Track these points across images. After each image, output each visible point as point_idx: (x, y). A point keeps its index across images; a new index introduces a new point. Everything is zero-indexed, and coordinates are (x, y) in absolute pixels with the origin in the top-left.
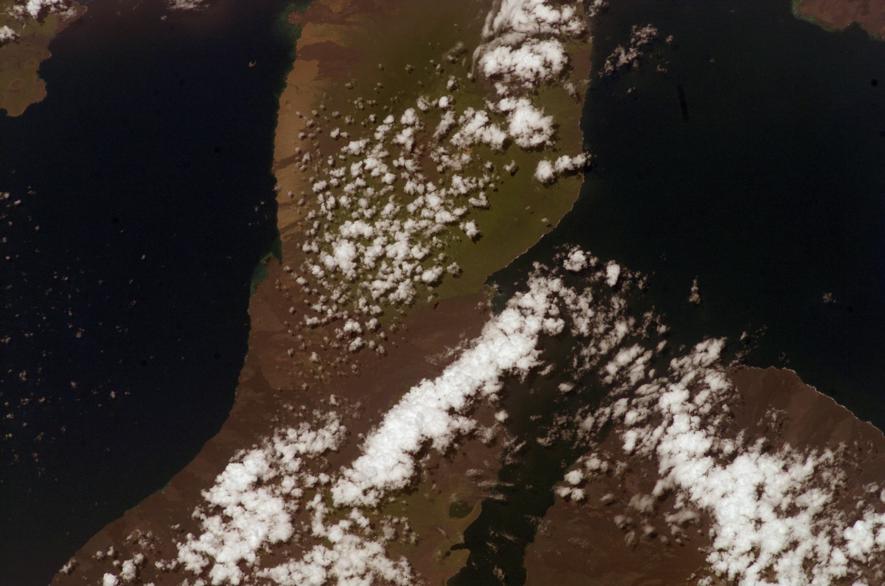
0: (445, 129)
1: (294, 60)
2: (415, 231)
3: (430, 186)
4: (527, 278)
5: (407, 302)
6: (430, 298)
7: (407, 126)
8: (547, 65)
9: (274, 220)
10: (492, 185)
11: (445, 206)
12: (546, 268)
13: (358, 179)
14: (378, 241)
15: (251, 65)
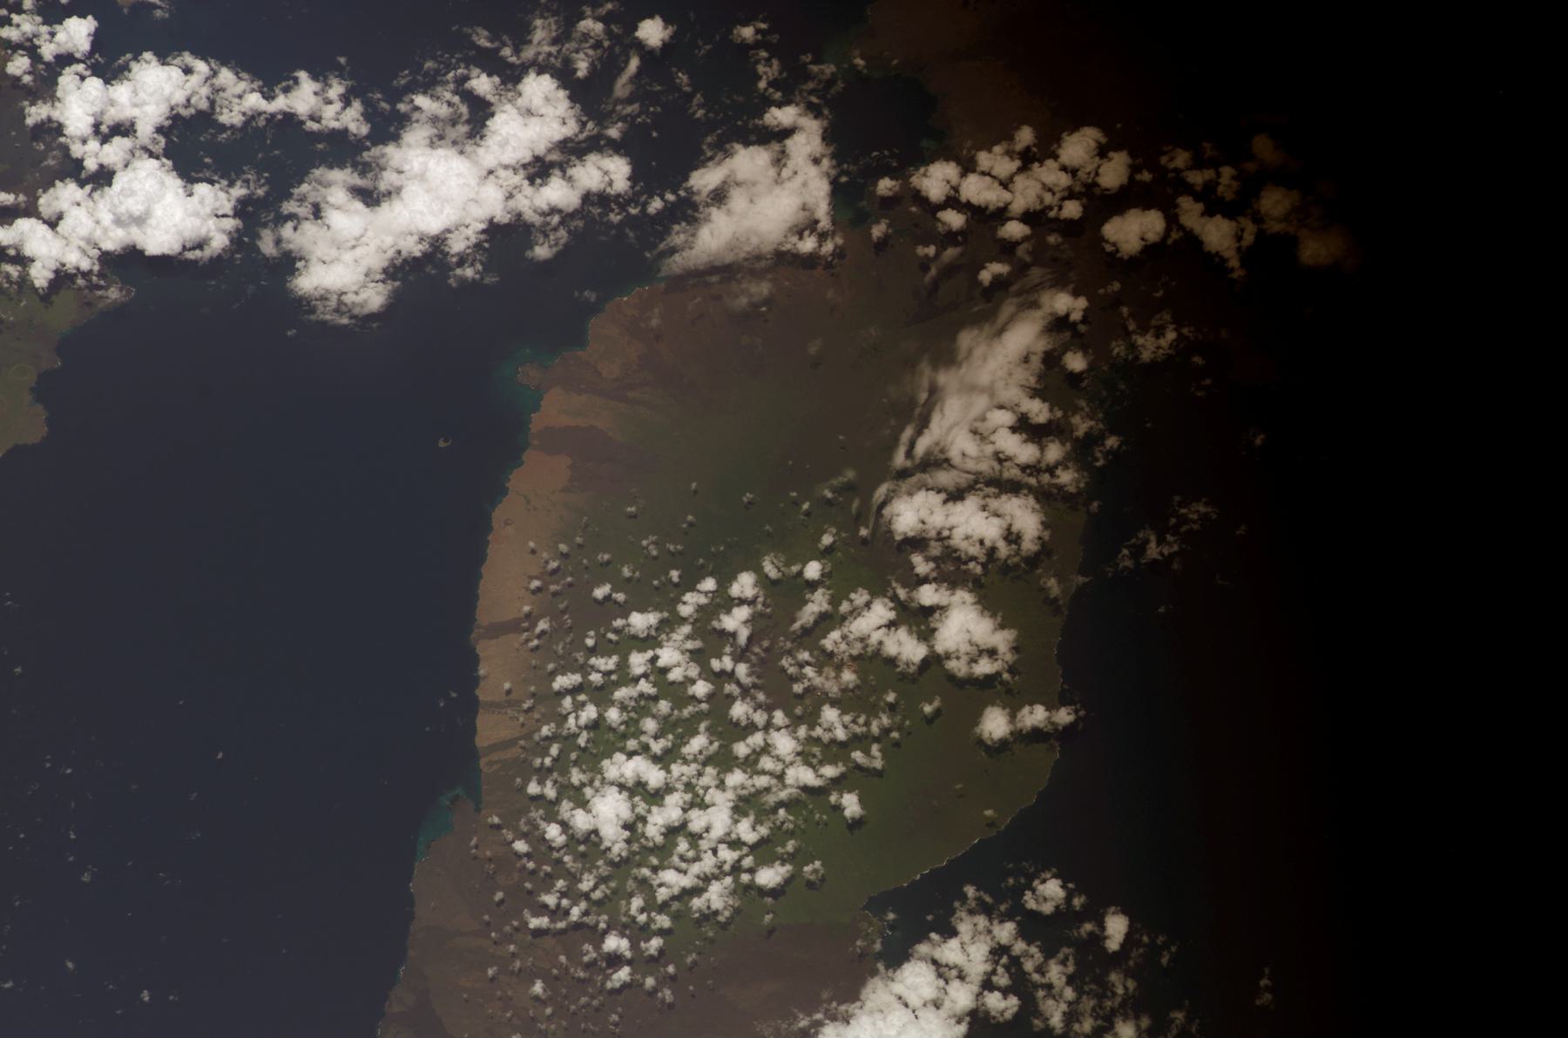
0: (812, 619)
1: (524, 450)
2: (745, 792)
3: (779, 717)
4: (953, 912)
5: (721, 919)
6: (768, 918)
7: (742, 602)
8: (1012, 537)
9: (472, 730)
10: (895, 735)
11: (805, 756)
12: (988, 899)
13: (643, 681)
14: (674, 801)
15: (442, 444)
